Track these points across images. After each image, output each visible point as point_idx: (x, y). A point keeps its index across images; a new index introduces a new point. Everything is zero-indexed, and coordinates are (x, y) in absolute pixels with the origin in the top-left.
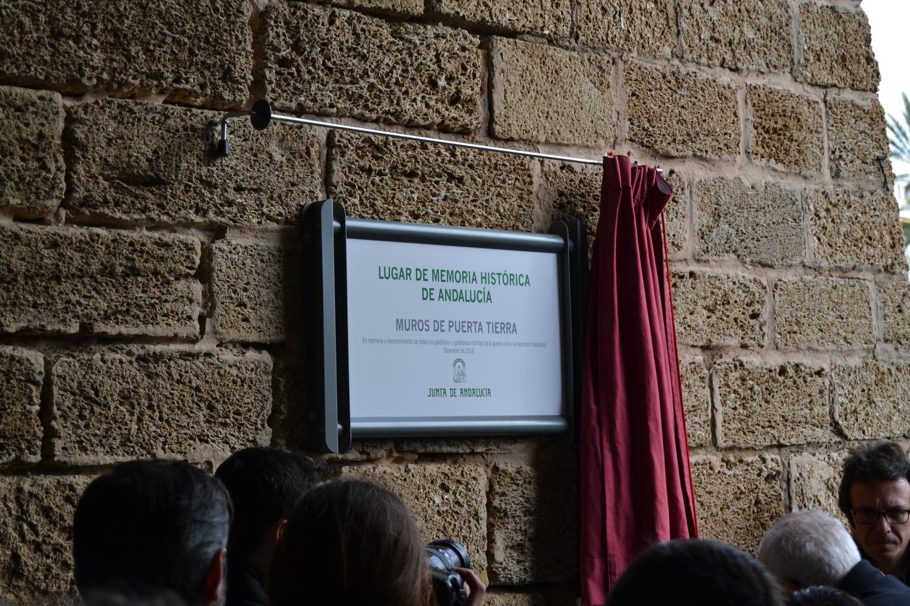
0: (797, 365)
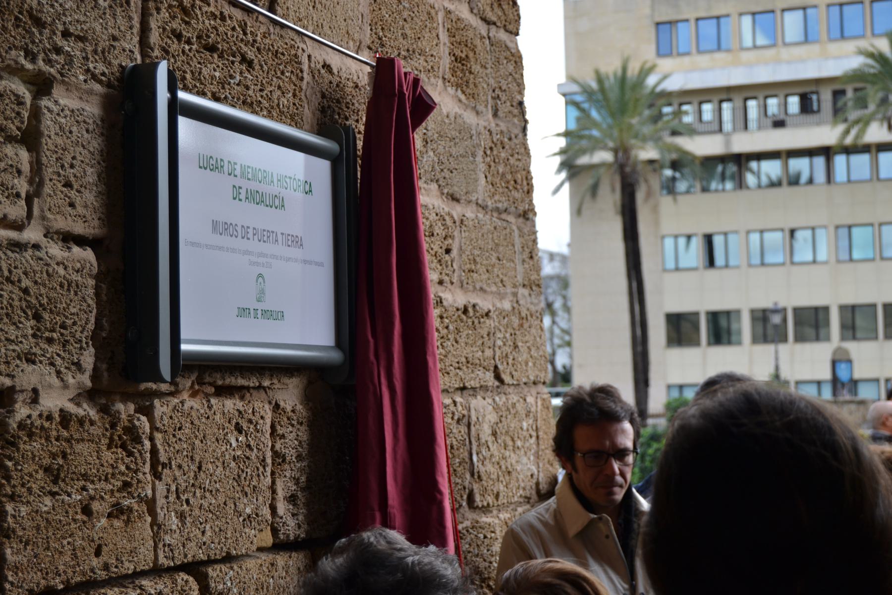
0: (474, 306)
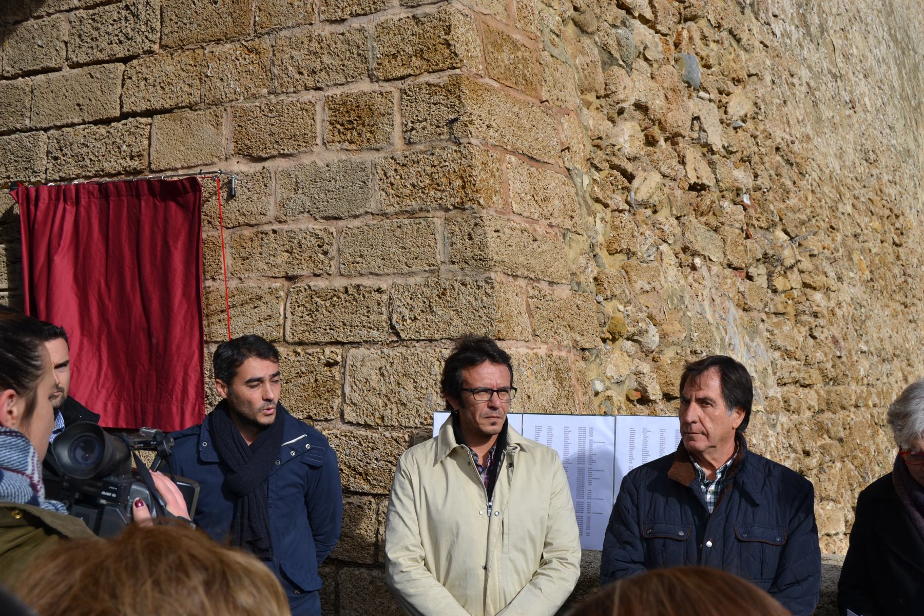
0: (358, 286)
